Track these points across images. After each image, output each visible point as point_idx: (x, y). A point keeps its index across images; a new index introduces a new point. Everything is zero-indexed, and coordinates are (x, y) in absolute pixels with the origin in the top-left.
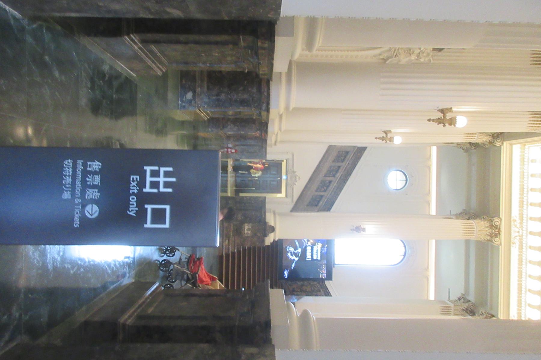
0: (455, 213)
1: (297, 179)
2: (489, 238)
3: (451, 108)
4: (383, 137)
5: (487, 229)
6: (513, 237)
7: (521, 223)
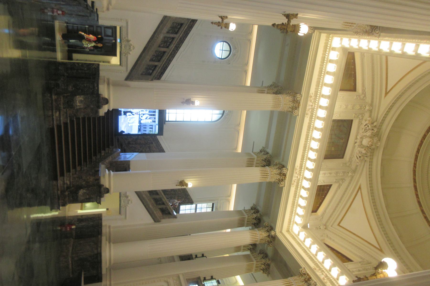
0: (267, 86)
1: (131, 49)
2: (290, 110)
3: (297, 15)
4: (219, 22)
5: (290, 103)
6: (307, 109)
7: (315, 99)
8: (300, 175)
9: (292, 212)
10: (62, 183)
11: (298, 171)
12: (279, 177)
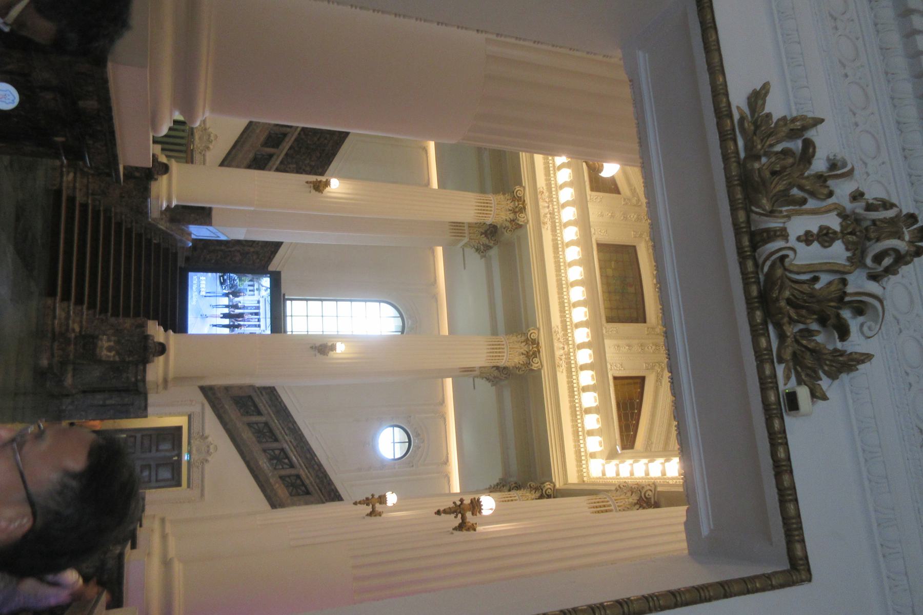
2: (512, 216)
5: (509, 202)
6: (542, 215)
7: (550, 197)
8: (568, 345)
9: (576, 433)
10: (63, 315)
11: (561, 334)
12: (526, 348)
